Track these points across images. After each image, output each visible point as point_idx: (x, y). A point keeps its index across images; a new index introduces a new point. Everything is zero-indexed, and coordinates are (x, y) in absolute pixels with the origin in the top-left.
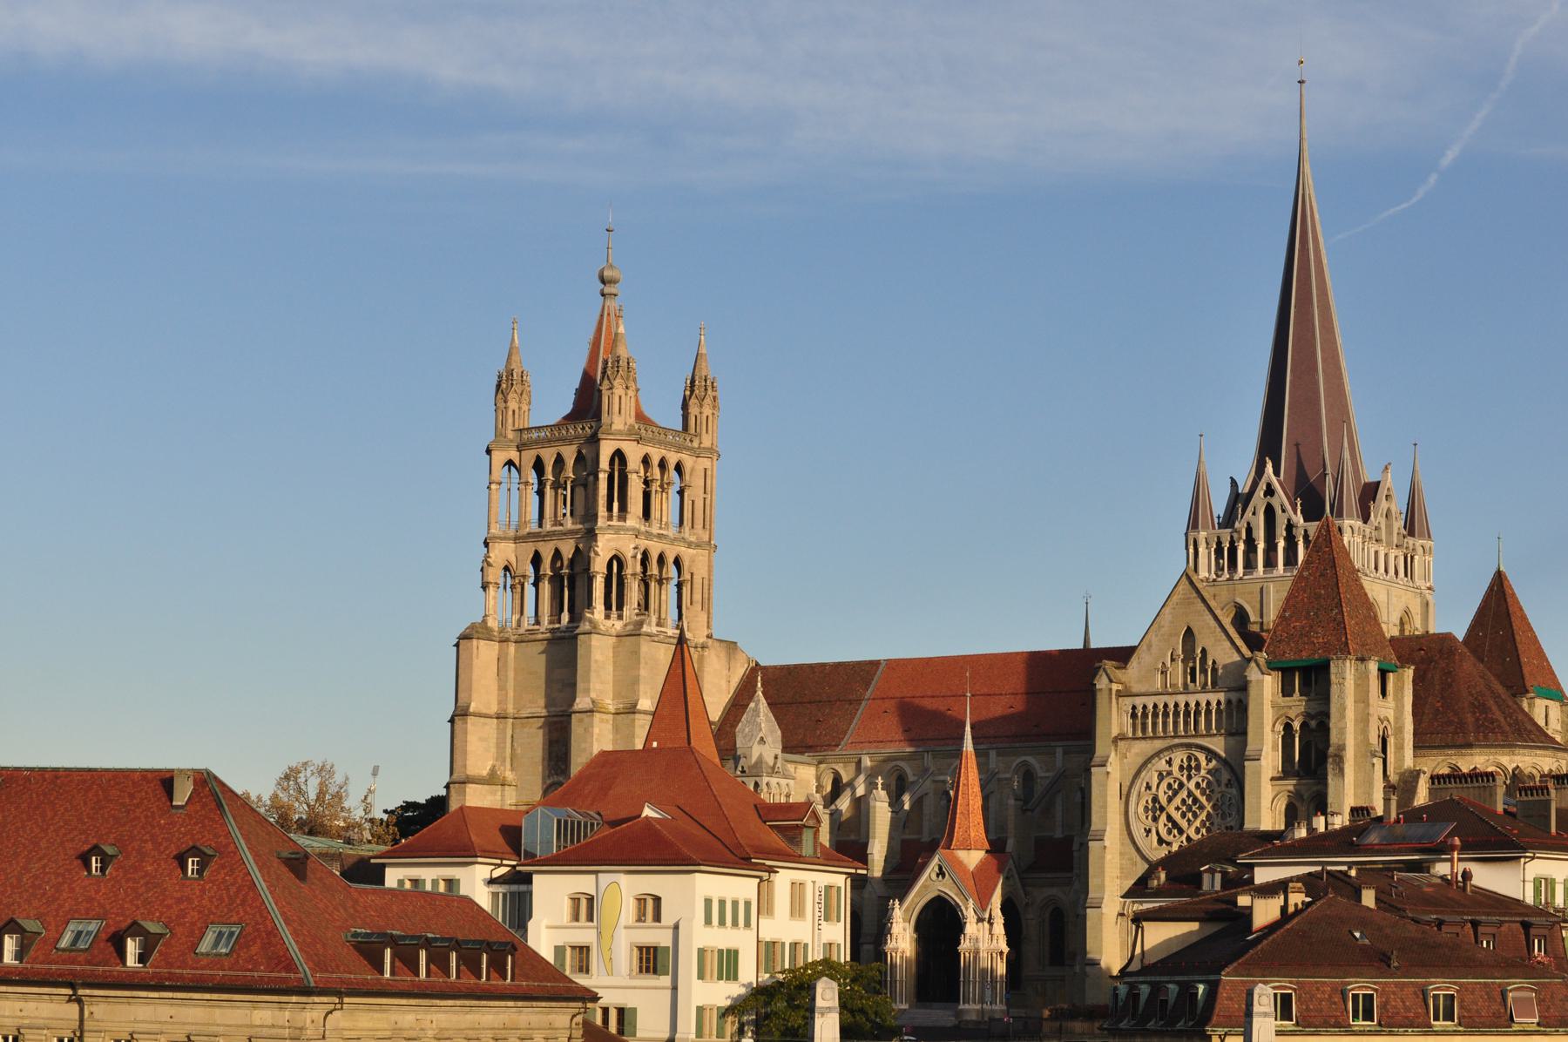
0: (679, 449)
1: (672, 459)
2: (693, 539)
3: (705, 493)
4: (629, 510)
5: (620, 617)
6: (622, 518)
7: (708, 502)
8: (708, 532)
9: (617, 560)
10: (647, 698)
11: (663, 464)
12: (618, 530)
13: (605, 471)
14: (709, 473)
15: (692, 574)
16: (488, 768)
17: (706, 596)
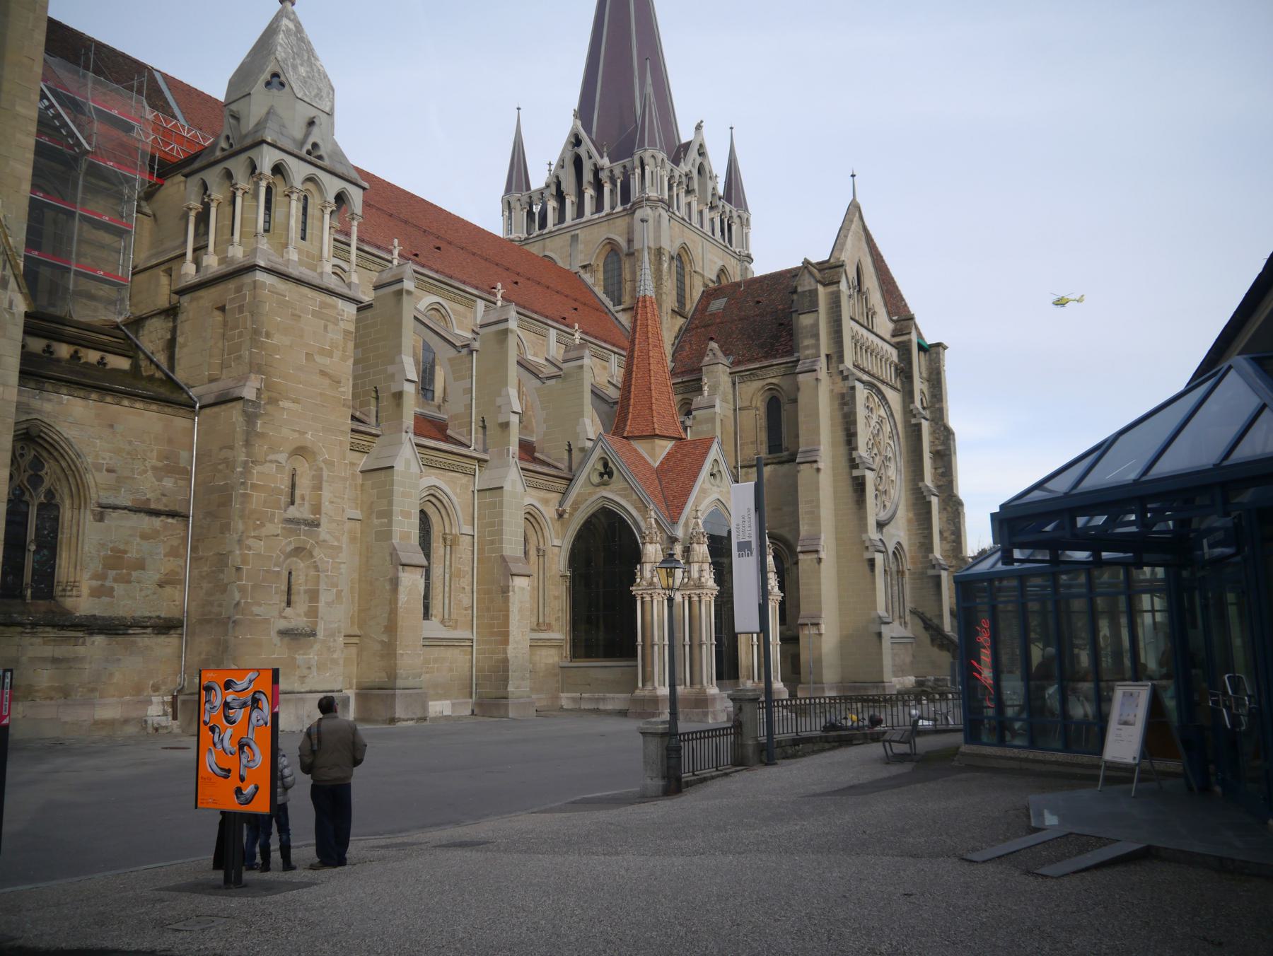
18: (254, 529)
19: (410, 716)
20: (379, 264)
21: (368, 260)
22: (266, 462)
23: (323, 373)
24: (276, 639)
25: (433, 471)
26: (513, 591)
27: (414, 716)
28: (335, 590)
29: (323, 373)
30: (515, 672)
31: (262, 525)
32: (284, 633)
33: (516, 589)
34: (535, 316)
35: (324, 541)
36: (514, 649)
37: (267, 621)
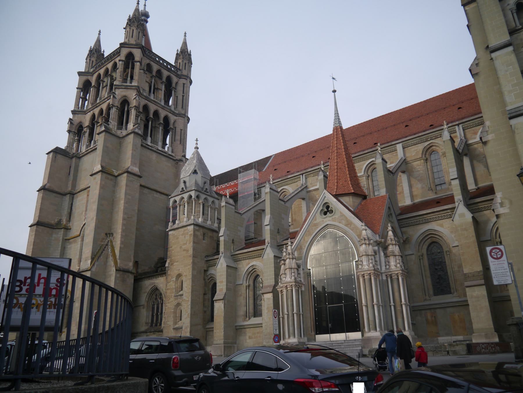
0: (169, 70)
1: (165, 73)
2: (177, 112)
3: (183, 93)
4: (134, 78)
5: (126, 129)
6: (131, 83)
7: (184, 98)
8: (184, 110)
9: (125, 102)
10: (136, 167)
11: (159, 72)
12: (126, 88)
13: (122, 61)
14: (185, 85)
15: (175, 128)
16: (56, 220)
17: (182, 138)
18: (168, 301)
19: (216, 354)
20: (298, 178)
21: (292, 180)
22: (170, 282)
23: (184, 250)
24: (172, 331)
25: (254, 259)
26: (264, 300)
27: (218, 354)
28: (187, 314)
29: (184, 250)
30: (266, 336)
31: (170, 299)
32: (174, 329)
33: (265, 300)
34: (366, 152)
35: (184, 299)
36: (266, 325)
37: (170, 325)
